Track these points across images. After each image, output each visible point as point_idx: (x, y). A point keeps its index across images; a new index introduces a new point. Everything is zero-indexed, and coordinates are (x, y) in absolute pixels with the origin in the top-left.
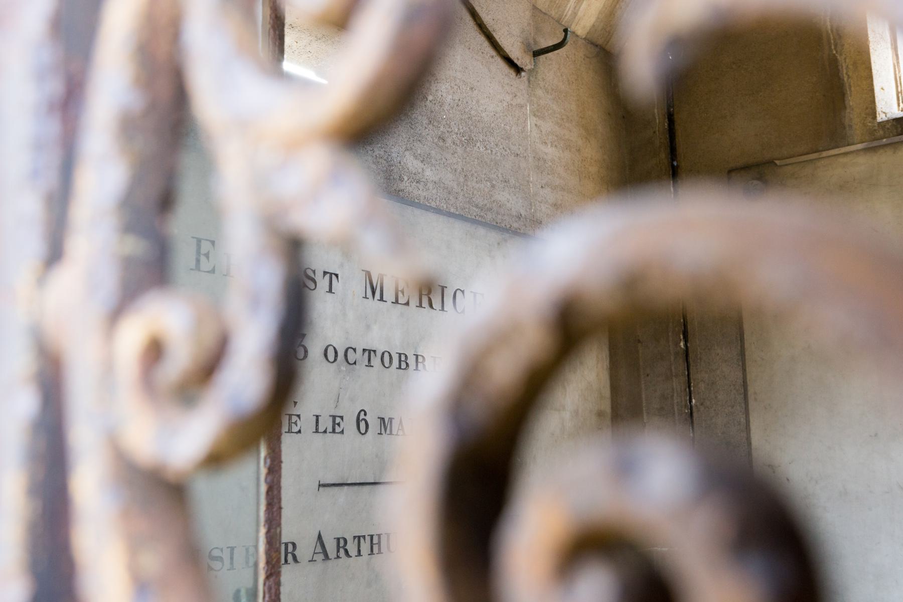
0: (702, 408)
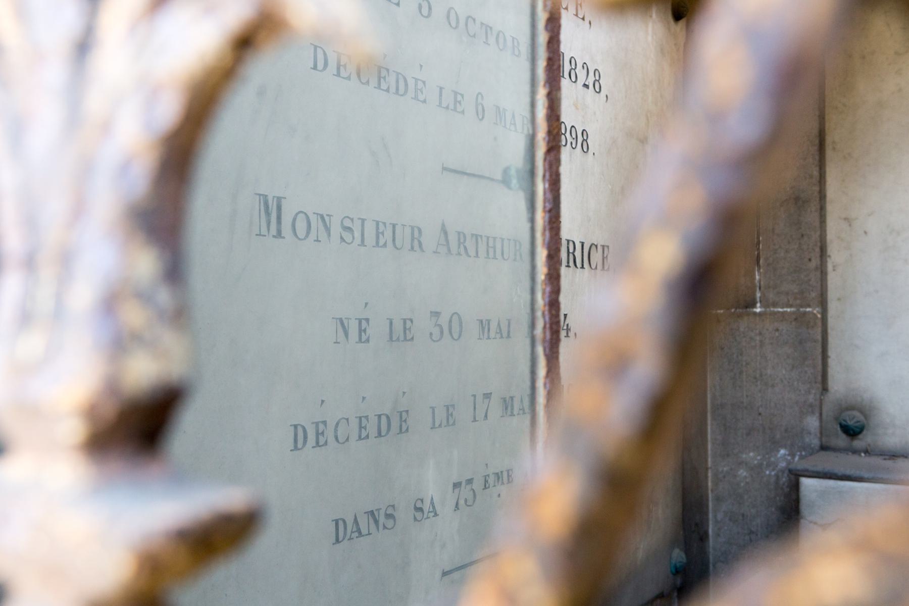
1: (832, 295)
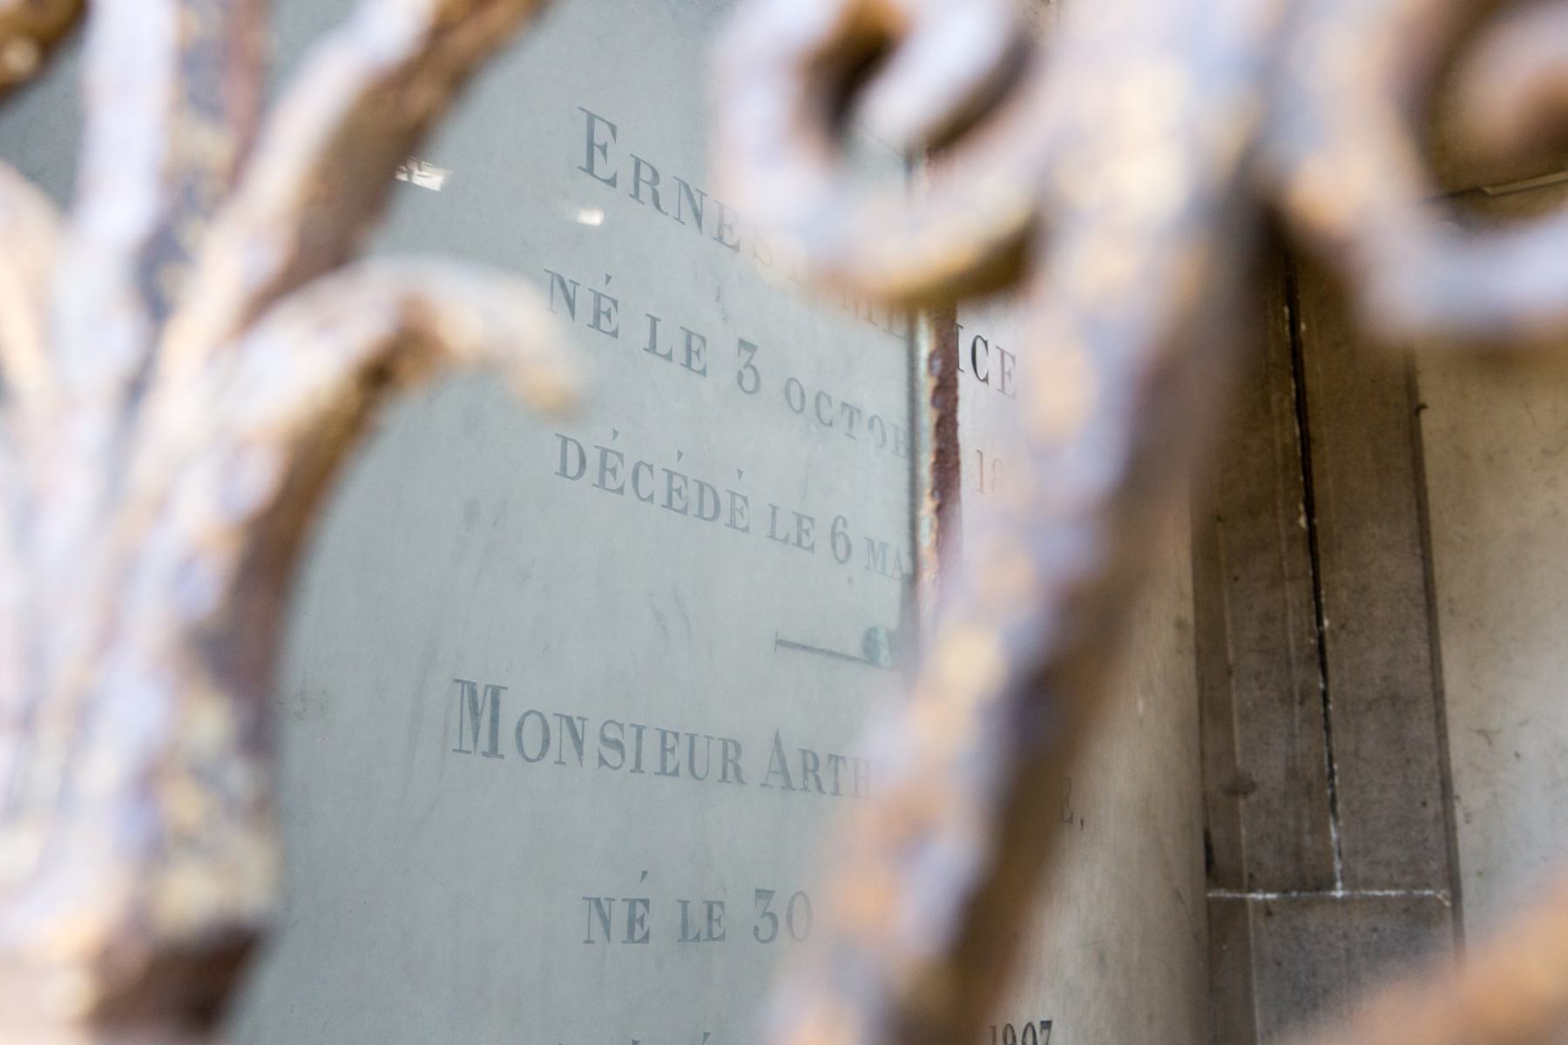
0: (1343, 635)
1: (1468, 865)
